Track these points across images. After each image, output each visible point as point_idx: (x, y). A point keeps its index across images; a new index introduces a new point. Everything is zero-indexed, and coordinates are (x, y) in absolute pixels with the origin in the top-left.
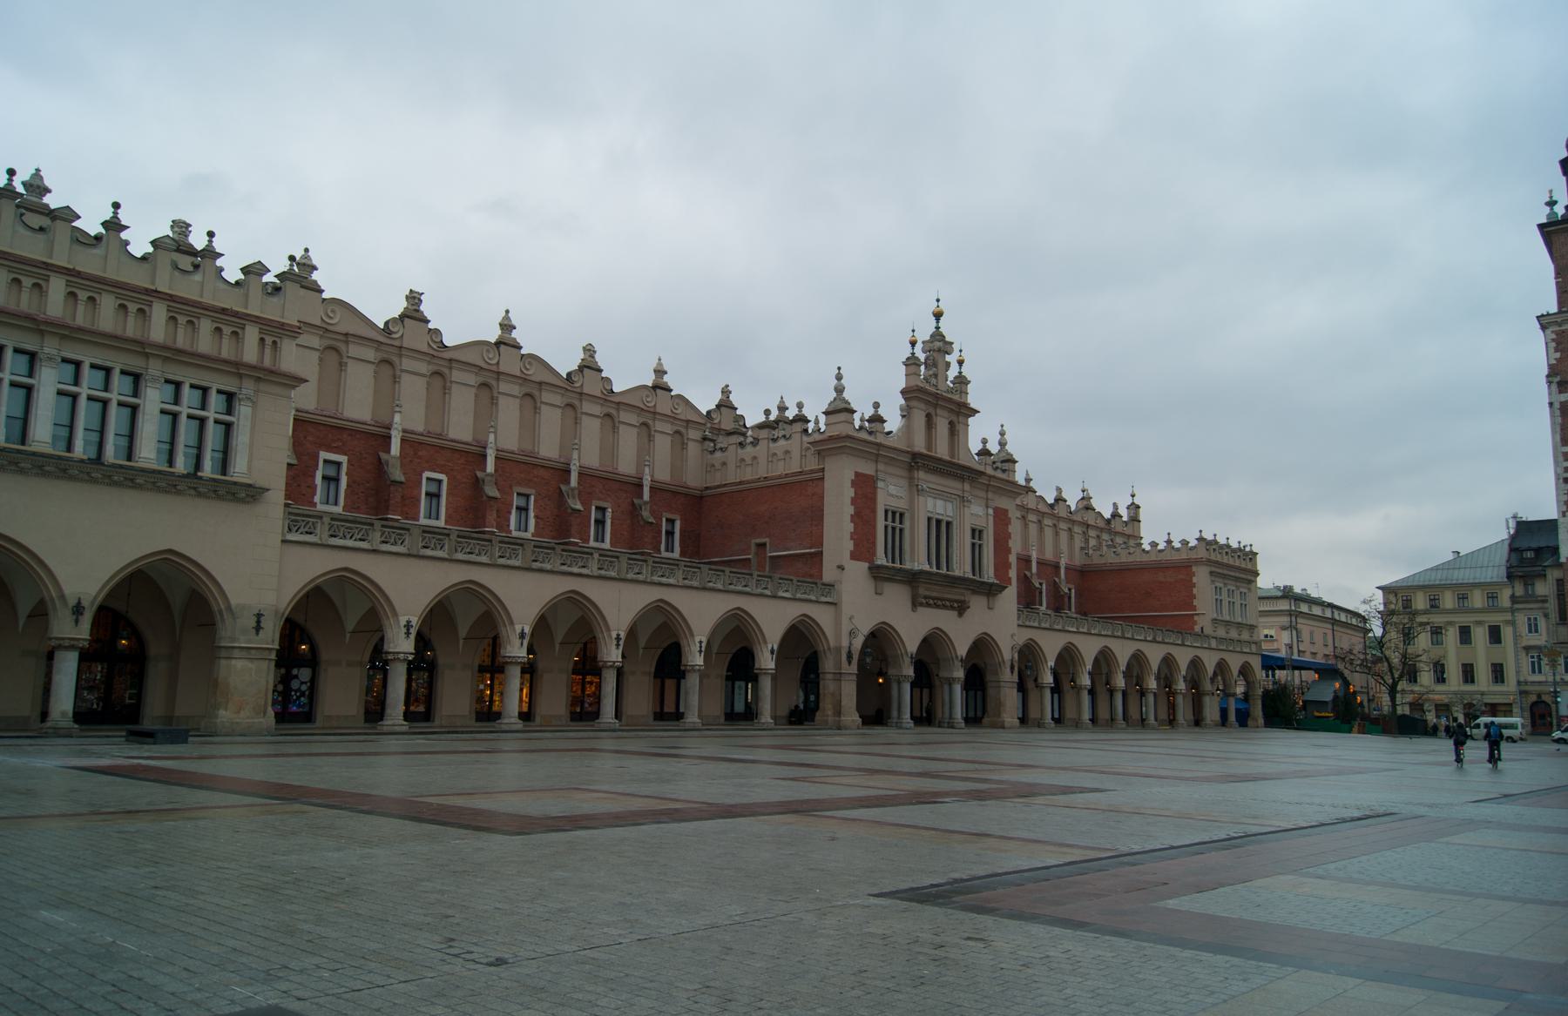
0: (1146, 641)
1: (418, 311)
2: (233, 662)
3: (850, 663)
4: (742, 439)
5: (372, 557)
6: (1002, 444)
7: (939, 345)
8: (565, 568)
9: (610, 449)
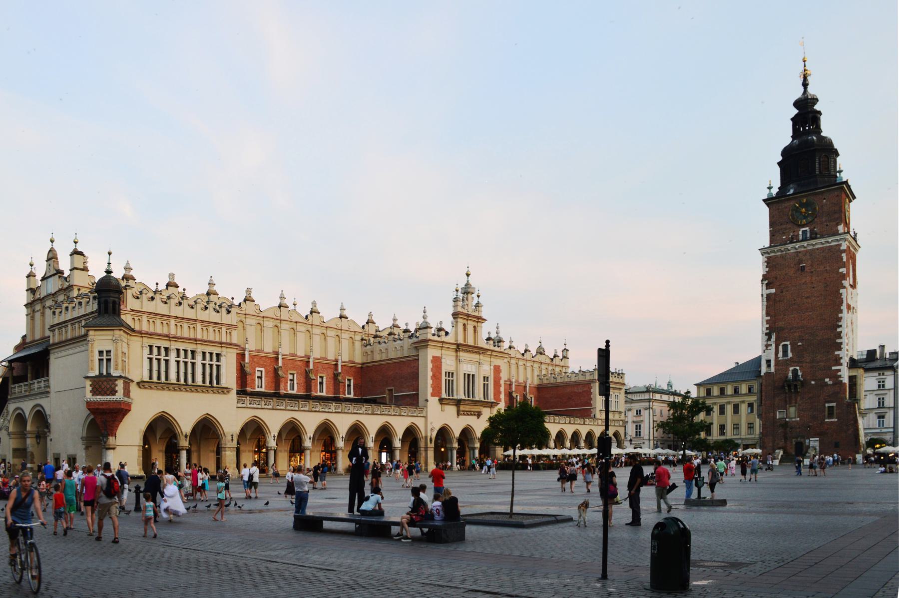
2: (226, 452)
3: (431, 443)
5: (262, 411)
7: (467, 290)
8: (323, 410)
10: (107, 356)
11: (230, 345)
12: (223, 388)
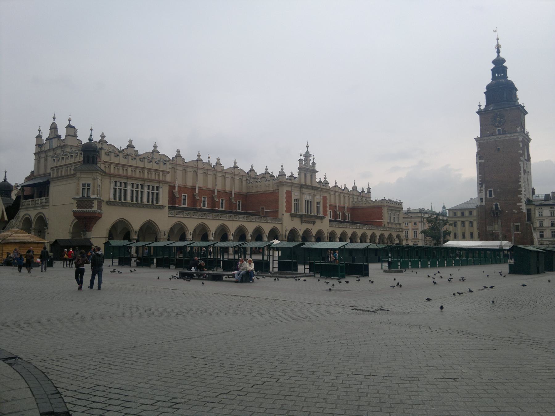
0: (366, 229)
1: (179, 154)
3: (285, 238)
4: (257, 180)
5: (184, 219)
6: (325, 178)
7: (308, 155)
9: (224, 185)
10: (88, 186)
11: (164, 182)
12: (160, 205)
